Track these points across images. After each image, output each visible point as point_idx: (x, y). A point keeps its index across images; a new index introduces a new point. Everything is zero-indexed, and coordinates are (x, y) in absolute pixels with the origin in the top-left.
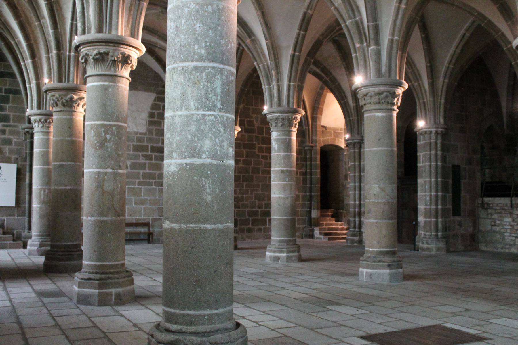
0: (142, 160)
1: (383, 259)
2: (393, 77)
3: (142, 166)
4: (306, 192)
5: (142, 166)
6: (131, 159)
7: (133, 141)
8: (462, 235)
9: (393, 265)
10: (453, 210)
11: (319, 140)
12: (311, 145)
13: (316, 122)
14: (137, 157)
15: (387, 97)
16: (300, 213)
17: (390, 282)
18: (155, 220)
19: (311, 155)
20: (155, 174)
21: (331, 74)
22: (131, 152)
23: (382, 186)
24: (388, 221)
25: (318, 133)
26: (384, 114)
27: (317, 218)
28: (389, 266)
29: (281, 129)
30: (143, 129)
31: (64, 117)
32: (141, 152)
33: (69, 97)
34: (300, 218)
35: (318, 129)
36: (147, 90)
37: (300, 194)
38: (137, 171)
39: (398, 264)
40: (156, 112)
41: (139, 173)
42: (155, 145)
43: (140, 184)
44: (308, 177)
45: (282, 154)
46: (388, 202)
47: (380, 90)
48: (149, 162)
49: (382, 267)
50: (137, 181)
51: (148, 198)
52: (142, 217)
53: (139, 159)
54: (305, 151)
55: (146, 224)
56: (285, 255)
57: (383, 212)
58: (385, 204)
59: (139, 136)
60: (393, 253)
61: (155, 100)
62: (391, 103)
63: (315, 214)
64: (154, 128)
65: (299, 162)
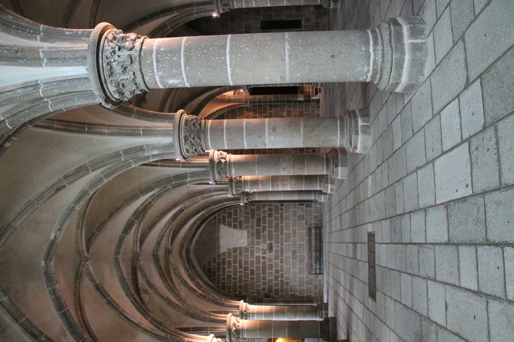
0: (266, 233)
1: (332, 170)
2: (208, 165)
3: (270, 232)
4: (285, 105)
5: (270, 232)
6: (266, 240)
7: (253, 239)
8: (316, 18)
9: (336, 163)
10: (295, 28)
11: (245, 96)
12: (249, 103)
13: (231, 100)
14: (264, 236)
15: (221, 169)
16: (301, 110)
17: (347, 166)
18: (306, 223)
19: (256, 102)
20: (275, 223)
21: (196, 108)
22: (261, 240)
23: (281, 170)
24: (306, 164)
25: (239, 98)
26: (233, 169)
27: (304, 96)
28: (336, 167)
29: (243, 187)
30: (245, 233)
31: (246, 334)
32: (260, 234)
33: (234, 333)
34: (304, 109)
35: (237, 98)
36: (219, 230)
37: (286, 110)
38: (274, 236)
39: (335, 159)
40: (233, 224)
41: (275, 235)
42: (255, 224)
43: (282, 234)
44: (273, 104)
45: (260, 186)
46: (293, 165)
47: (217, 173)
48: (267, 228)
49: (337, 171)
50: (280, 236)
51: (292, 228)
52: (305, 232)
53: (265, 235)
54: (253, 106)
55: (310, 229)
56: (329, 185)
57: (300, 169)
58: (294, 168)
59: (250, 235)
60: (328, 160)
61: (225, 225)
62: (225, 165)
63: (301, 98)
64: (244, 225)
65: (263, 111)
